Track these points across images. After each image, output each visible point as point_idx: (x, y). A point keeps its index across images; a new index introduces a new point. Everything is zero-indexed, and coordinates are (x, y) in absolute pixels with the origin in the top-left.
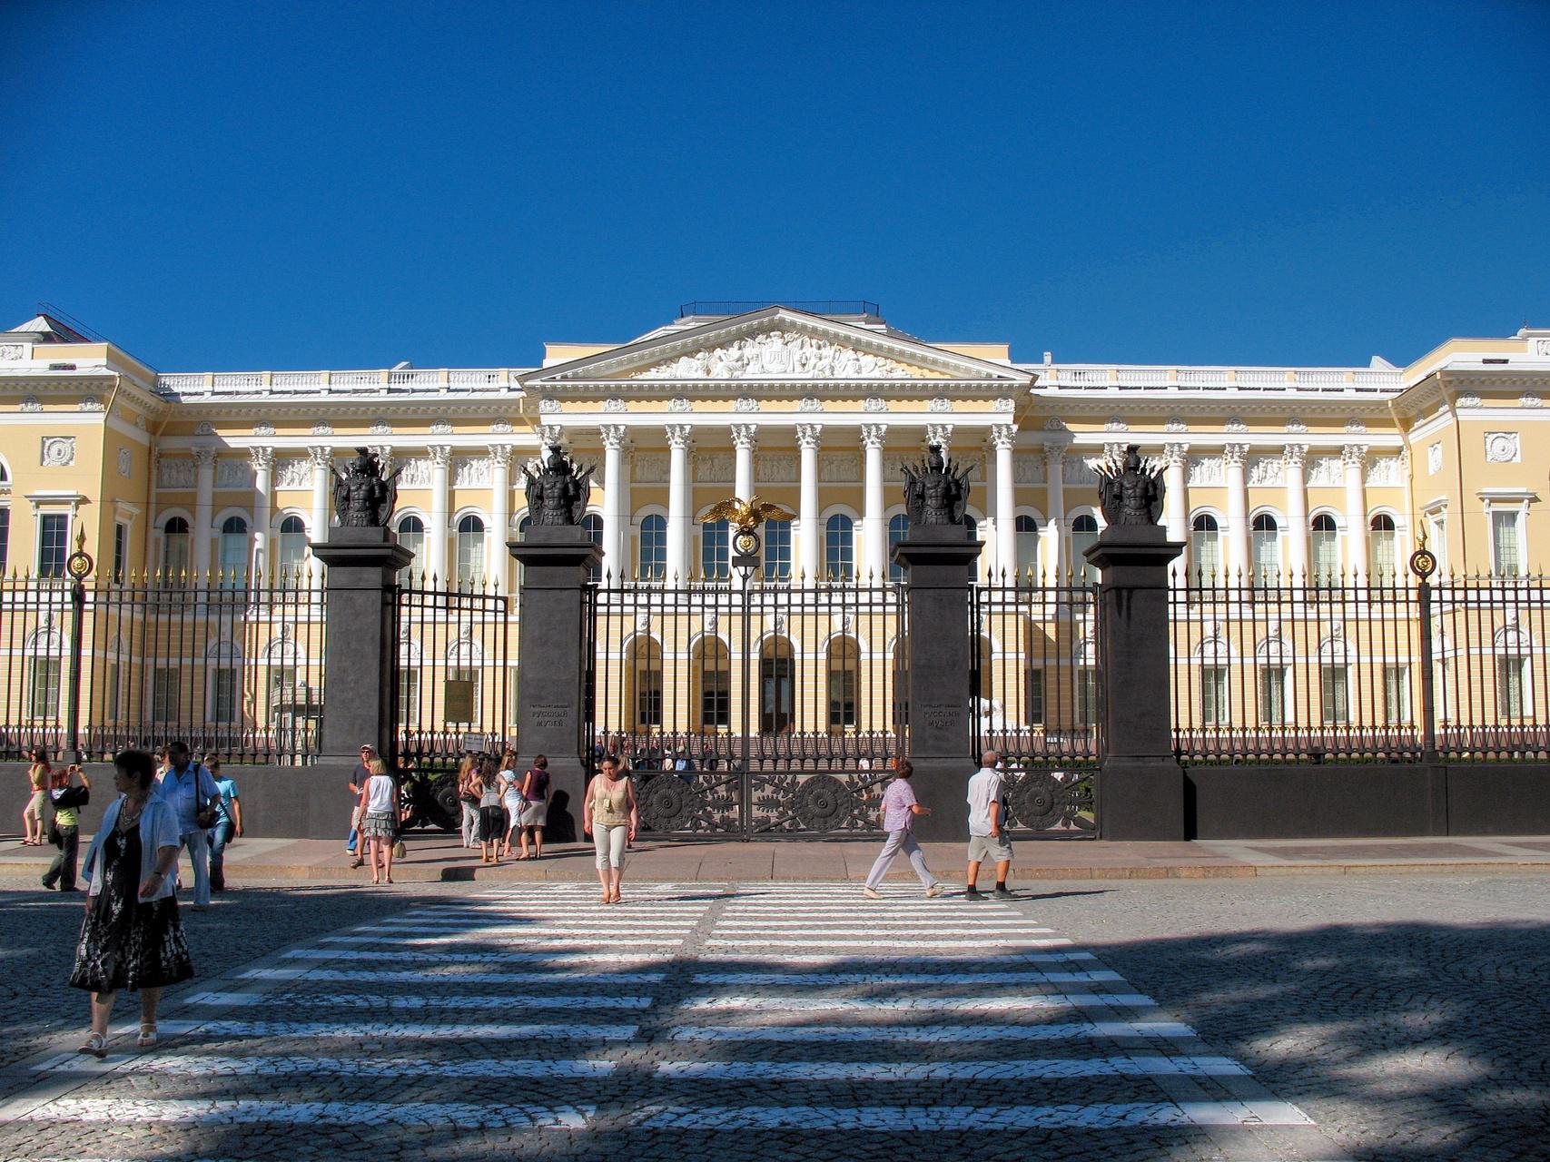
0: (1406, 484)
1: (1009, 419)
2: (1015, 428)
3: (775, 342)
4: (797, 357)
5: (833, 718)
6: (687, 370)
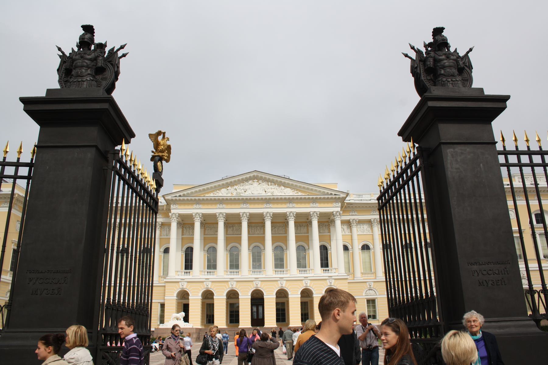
1: (339, 209)
3: (255, 184)
5: (278, 320)
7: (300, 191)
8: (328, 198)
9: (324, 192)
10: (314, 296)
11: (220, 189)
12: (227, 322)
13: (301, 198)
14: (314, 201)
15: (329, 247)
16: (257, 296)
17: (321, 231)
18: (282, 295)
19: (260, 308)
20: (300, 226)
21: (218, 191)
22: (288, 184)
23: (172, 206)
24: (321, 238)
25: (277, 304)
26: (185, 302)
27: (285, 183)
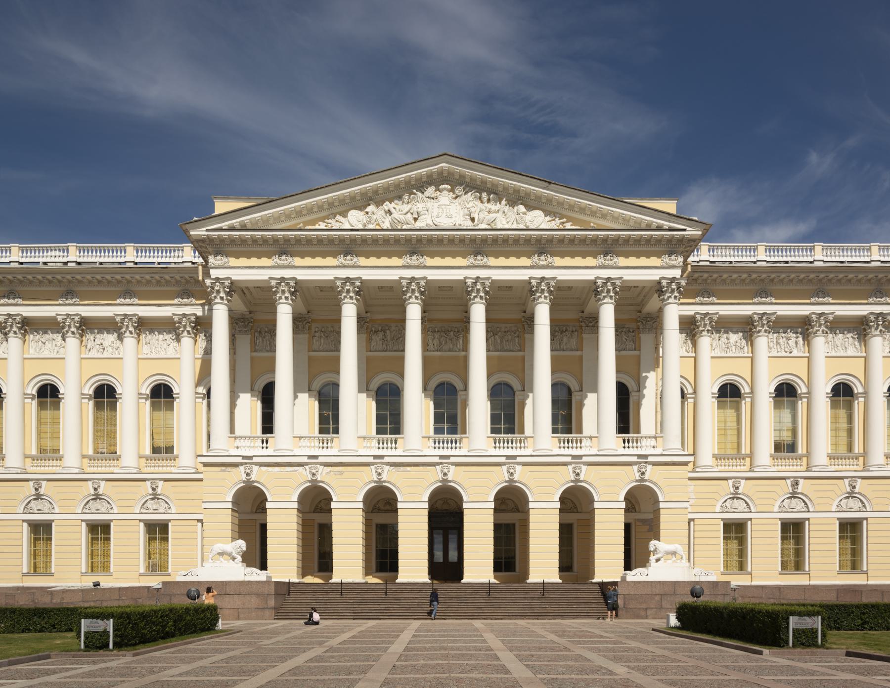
1: (677, 273)
3: (445, 197)
11: (344, 214)
14: (609, 247)
16: (445, 507)
21: (338, 217)
22: (538, 198)
27: (528, 194)
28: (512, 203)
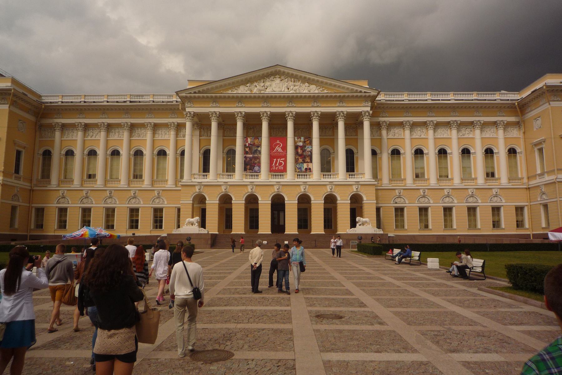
0: (521, 136)
1: (368, 109)
2: (371, 112)
3: (278, 81)
4: (286, 86)
5: (300, 227)
6: (243, 90)
7: (326, 88)
8: (357, 96)
9: (352, 89)
10: (338, 202)
12: (245, 228)
13: (327, 97)
14: (341, 99)
15: (355, 151)
17: (348, 134)
18: (304, 202)
19: (281, 214)
20: (326, 129)
21: (236, 88)
22: (313, 80)
23: (186, 104)
24: (347, 141)
25: (299, 210)
26: (202, 206)
28: (303, 82)
